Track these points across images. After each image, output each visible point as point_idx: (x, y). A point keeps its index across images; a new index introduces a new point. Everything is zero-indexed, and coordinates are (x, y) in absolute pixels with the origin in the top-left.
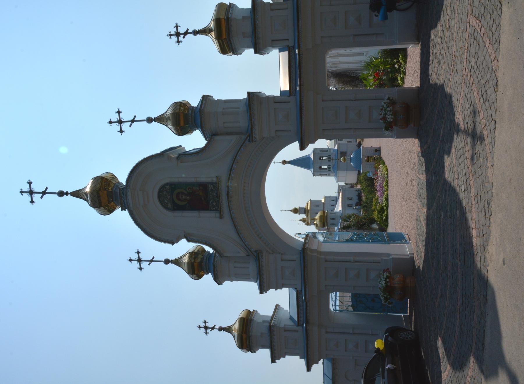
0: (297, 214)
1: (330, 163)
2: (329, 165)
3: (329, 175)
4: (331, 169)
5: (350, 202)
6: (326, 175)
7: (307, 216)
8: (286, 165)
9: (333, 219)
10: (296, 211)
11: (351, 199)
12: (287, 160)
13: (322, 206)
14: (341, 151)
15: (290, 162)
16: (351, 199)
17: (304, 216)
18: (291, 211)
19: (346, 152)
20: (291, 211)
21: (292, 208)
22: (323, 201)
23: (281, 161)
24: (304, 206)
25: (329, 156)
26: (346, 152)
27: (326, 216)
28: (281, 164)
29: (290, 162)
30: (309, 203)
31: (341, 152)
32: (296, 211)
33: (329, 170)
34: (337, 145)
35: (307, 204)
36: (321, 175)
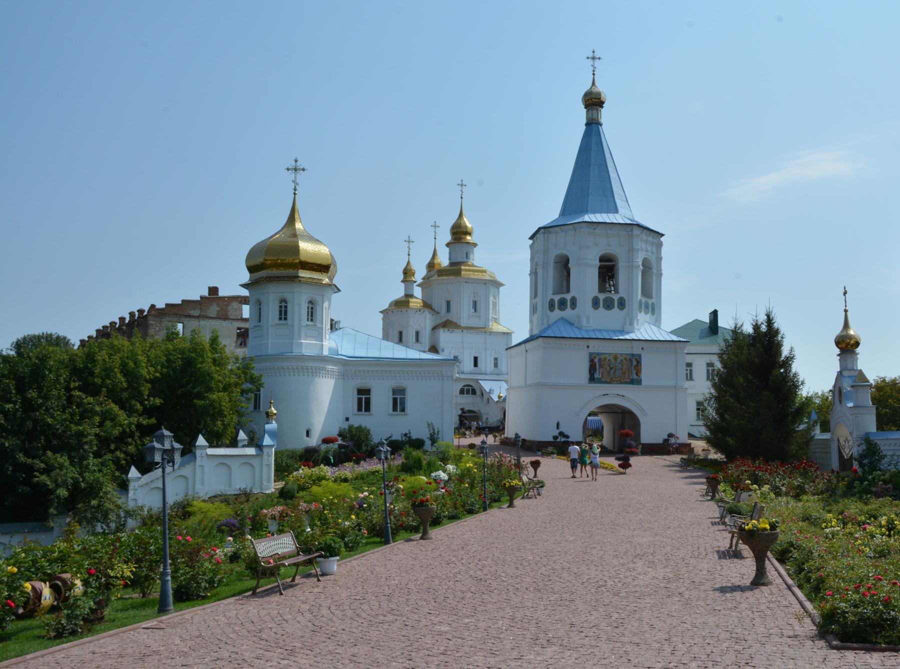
0: (448, 238)
1: (585, 304)
2: (574, 302)
3: (534, 309)
4: (557, 314)
5: (381, 400)
6: (534, 293)
7: (442, 272)
8: (584, 111)
9: (283, 314)
10: (459, 233)
11: (398, 404)
12: (605, 115)
13: (473, 322)
15: (593, 125)
16: (398, 404)
17: (444, 260)
18: (461, 215)
20: (461, 215)
22: (495, 327)
23: (601, 87)
24: (480, 258)
25: (622, 304)
26: (639, 382)
27: (295, 278)
28: (587, 87)
29: (593, 125)
30: (487, 277)
31: (640, 356)
32: (459, 233)
33: (551, 306)
34: (675, 338)
35: (485, 272)
36: (534, 273)
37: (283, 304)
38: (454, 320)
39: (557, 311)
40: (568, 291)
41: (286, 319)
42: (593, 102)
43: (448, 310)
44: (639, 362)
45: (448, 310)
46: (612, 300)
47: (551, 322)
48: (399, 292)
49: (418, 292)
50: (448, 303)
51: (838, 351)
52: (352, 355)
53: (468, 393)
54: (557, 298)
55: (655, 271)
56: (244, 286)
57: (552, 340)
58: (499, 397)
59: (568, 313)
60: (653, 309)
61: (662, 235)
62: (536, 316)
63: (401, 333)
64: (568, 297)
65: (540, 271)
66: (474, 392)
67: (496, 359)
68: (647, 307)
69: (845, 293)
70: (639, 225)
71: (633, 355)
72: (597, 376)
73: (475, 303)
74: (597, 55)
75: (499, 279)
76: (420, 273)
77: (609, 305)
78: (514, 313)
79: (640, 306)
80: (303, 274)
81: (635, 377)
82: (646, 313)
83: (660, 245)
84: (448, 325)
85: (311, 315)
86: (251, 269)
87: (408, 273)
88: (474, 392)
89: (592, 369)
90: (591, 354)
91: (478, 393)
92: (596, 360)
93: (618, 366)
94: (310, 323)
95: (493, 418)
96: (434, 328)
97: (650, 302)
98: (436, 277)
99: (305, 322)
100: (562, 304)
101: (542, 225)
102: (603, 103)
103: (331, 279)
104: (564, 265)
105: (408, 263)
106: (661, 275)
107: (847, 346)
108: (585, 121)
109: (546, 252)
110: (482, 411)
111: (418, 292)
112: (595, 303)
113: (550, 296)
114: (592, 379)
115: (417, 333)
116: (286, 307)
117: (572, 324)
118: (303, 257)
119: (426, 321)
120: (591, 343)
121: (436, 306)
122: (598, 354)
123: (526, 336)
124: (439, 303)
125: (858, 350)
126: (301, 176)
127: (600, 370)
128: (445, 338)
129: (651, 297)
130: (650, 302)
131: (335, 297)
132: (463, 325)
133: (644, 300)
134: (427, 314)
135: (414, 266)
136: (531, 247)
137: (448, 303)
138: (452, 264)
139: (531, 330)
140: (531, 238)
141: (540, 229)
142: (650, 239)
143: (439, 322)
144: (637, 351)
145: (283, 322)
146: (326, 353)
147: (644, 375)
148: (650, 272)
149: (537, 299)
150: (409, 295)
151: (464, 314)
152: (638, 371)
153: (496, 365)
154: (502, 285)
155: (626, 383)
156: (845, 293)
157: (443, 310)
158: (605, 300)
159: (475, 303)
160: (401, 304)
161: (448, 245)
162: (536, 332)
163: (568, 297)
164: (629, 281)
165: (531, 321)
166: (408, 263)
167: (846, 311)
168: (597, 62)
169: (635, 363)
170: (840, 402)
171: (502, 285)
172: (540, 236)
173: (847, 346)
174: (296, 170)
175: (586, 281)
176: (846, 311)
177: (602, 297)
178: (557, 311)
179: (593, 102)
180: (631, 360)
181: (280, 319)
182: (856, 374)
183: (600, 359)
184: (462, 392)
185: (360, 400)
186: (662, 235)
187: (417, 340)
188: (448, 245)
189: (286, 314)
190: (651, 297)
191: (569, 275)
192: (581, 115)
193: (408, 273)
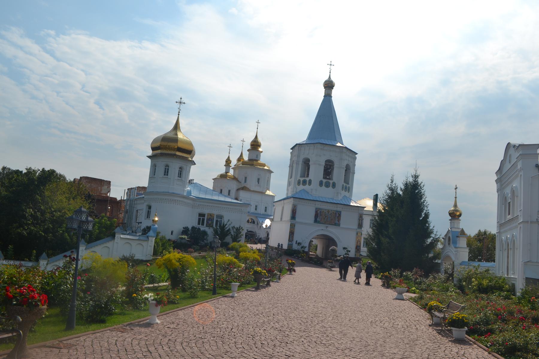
2: (310, 182)
3: (289, 184)
4: (301, 187)
6: (291, 176)
7: (244, 163)
9: (166, 172)
12: (335, 92)
14: (343, 214)
15: (328, 96)
17: (246, 158)
18: (256, 137)
19: (338, 225)
20: (256, 137)
21: (260, 139)
22: (268, 192)
25: (334, 185)
26: (339, 225)
29: (328, 96)
31: (340, 212)
32: (255, 145)
36: (291, 166)
37: (167, 168)
38: (248, 186)
39: (301, 185)
40: (308, 176)
41: (167, 175)
42: (329, 85)
43: (245, 182)
44: (340, 215)
45: (245, 182)
46: (329, 183)
47: (298, 191)
48: (223, 171)
49: (231, 172)
50: (246, 178)
51: (450, 218)
52: (198, 196)
53: (251, 222)
54: (302, 179)
55: (351, 171)
56: (149, 157)
57: (298, 200)
58: (266, 226)
59: (307, 187)
60: (349, 190)
61: (357, 154)
62: (290, 187)
63: (221, 190)
64: (308, 179)
65: (295, 165)
66: (254, 222)
67: (266, 208)
68: (346, 188)
69: (456, 189)
70: (346, 148)
71: (337, 211)
72: (318, 219)
73: (259, 179)
74: (332, 64)
75: (272, 169)
76: (234, 162)
77: (327, 185)
78: (279, 186)
79: (343, 188)
80: (178, 153)
81: (337, 222)
82: (346, 191)
83: (355, 158)
84: (244, 188)
85: (180, 175)
86: (153, 149)
87: (228, 162)
88: (254, 222)
89: (316, 216)
90: (316, 209)
91: (256, 223)
92: (319, 212)
93: (328, 216)
94: (179, 178)
95: (263, 236)
96: (238, 190)
97: (348, 186)
98: (241, 165)
99: (177, 177)
100: (304, 183)
101: (298, 143)
102: (333, 86)
103: (192, 158)
104: (307, 163)
105: (229, 157)
106: (354, 173)
107: (455, 215)
108: (324, 95)
109: (298, 156)
110: (257, 232)
111: (231, 172)
112: (321, 184)
113: (299, 178)
114: (316, 221)
115: (229, 191)
116: (168, 169)
117: (308, 193)
118: (180, 145)
119: (234, 186)
120: (317, 203)
121: (240, 179)
122: (320, 209)
123: (285, 196)
124: (241, 179)
125: (460, 218)
126: (182, 106)
127: (320, 217)
128: (242, 194)
129: (348, 184)
130: (348, 186)
131: (192, 167)
132: (252, 189)
133: (345, 184)
134: (235, 182)
135: (231, 159)
136: (291, 153)
137: (246, 178)
138: (249, 160)
139: (287, 194)
140: (291, 149)
141: (297, 144)
142: (351, 155)
143: (240, 187)
144: (339, 209)
145: (166, 176)
146: (185, 194)
147: (342, 222)
148: (349, 171)
149: (292, 179)
150: (227, 172)
151: (252, 184)
152: (339, 220)
153: (266, 211)
154: (273, 172)
155: (332, 225)
156: (456, 189)
157: (243, 182)
158: (326, 183)
159: (259, 179)
160: (223, 176)
161: (248, 150)
162: (290, 195)
163: (308, 179)
164: (338, 175)
165: (288, 190)
166: (229, 157)
167: (456, 198)
168: (332, 66)
169: (338, 215)
170: (449, 244)
171: (273, 172)
172: (296, 148)
173: (455, 215)
174: (180, 103)
175: (316, 173)
176: (456, 198)
177: (324, 181)
178: (301, 185)
179: (329, 85)
180: (336, 214)
181: (165, 175)
182: (459, 230)
183: (320, 212)
184: (248, 221)
185: (199, 219)
186: (357, 154)
187: (229, 194)
188: (248, 150)
189: (168, 171)
190: (348, 184)
191: (309, 169)
192: (321, 92)
193: (228, 162)
